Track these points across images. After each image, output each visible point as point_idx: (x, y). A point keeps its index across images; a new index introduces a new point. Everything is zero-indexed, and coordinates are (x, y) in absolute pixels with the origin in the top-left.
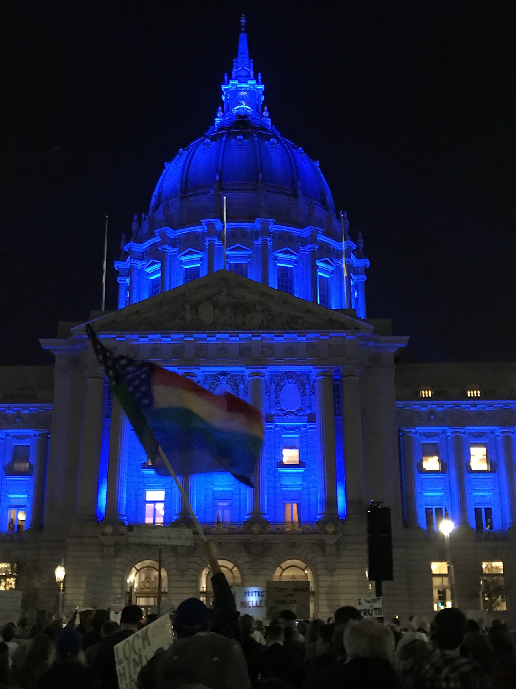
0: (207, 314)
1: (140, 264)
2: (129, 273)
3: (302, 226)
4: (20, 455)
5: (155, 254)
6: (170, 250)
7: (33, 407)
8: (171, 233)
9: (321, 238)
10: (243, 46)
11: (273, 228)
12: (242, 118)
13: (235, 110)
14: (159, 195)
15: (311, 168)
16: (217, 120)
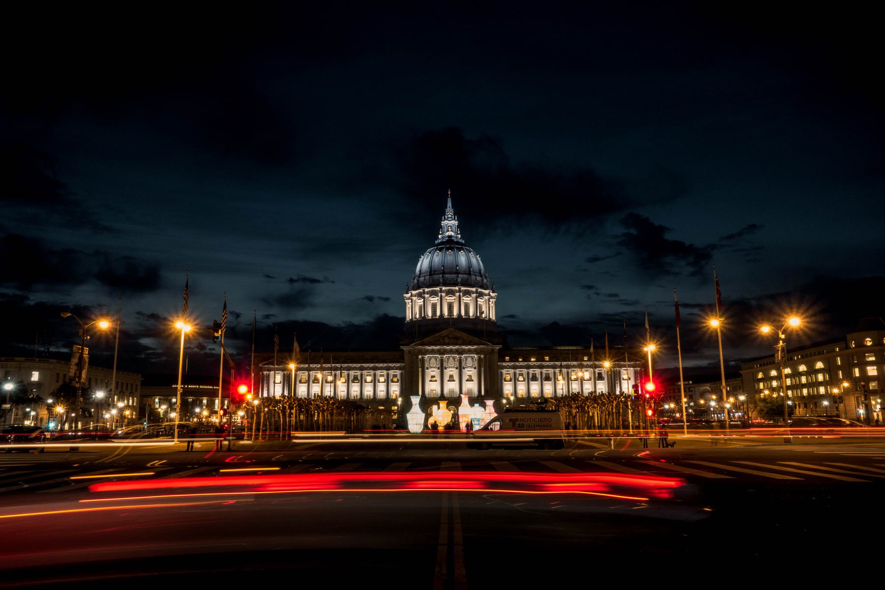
0: (447, 340)
1: (414, 298)
2: (409, 299)
3: (473, 287)
4: (395, 376)
5: (420, 296)
6: (426, 296)
7: (399, 365)
8: (426, 290)
9: (480, 290)
10: (449, 204)
11: (463, 288)
12: (450, 237)
13: (447, 234)
14: (420, 271)
15: (476, 261)
16: (440, 236)
